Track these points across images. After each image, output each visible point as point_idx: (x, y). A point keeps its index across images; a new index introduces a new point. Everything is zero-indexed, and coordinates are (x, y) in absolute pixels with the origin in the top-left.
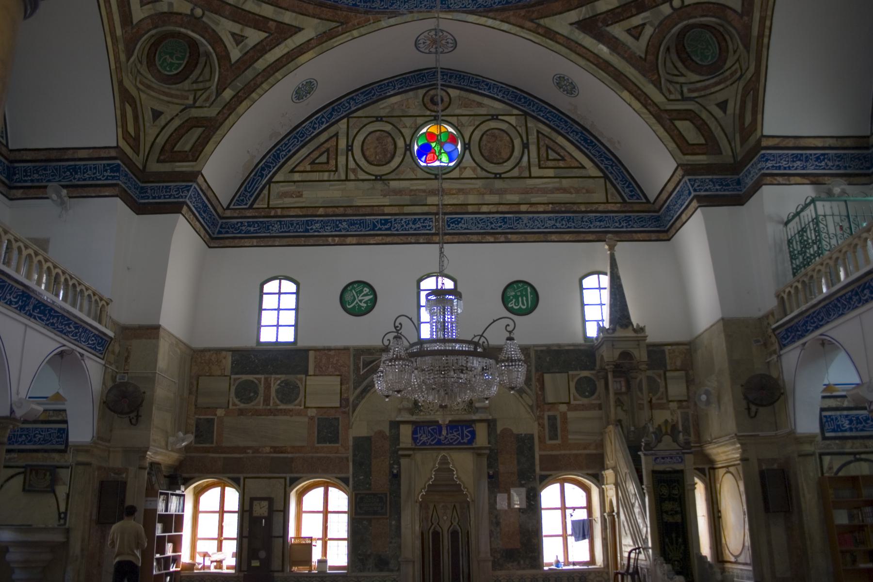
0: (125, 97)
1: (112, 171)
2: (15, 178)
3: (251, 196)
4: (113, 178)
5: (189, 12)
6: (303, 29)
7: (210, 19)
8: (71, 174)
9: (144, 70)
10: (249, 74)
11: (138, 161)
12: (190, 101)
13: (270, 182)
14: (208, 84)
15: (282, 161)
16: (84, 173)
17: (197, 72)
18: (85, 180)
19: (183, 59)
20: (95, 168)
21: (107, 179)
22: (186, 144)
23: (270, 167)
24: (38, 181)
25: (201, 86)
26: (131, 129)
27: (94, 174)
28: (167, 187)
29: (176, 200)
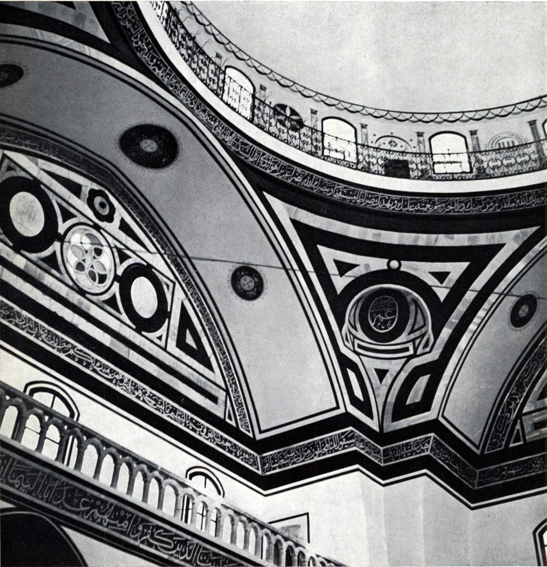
0: (345, 363)
1: (347, 439)
2: (266, 467)
3: (504, 435)
4: (349, 445)
5: (386, 267)
6: (504, 245)
7: (408, 266)
8: (311, 450)
9: (360, 334)
10: (462, 308)
11: (374, 424)
12: (411, 352)
13: (520, 415)
14: (423, 330)
15: (527, 389)
16: (323, 448)
17: (411, 322)
18: (324, 454)
19: (394, 313)
20: (331, 440)
21: (344, 448)
22: (416, 394)
23: (516, 399)
24: (285, 465)
25: (418, 334)
26: (358, 393)
27: (332, 446)
28: (407, 444)
29: (418, 456)
